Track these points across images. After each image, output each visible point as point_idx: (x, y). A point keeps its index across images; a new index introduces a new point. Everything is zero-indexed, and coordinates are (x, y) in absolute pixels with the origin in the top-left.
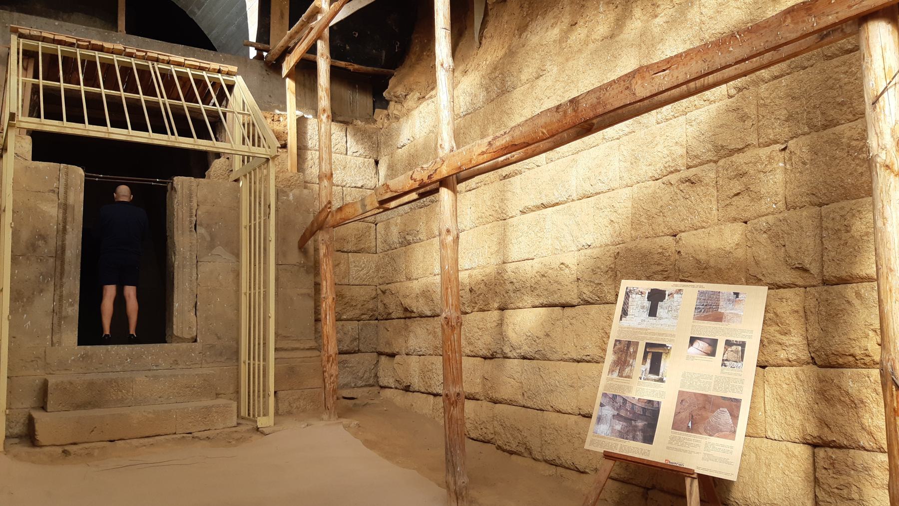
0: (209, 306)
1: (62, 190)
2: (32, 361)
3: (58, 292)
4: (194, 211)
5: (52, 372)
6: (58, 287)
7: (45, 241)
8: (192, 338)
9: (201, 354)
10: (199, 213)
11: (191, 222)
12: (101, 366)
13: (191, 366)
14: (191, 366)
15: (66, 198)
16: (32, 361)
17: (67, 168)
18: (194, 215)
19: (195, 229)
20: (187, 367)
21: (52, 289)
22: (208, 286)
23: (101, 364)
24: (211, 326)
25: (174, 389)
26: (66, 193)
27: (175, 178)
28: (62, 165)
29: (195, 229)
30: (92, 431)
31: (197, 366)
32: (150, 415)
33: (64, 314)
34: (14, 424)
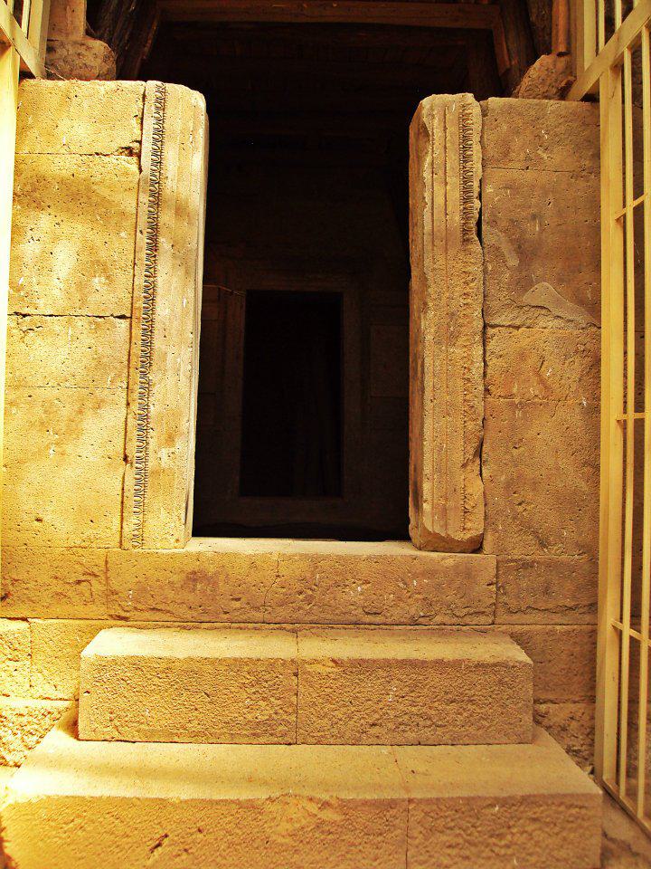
0: (515, 452)
1: (147, 148)
2: (79, 582)
3: (135, 407)
4: (476, 184)
5: (123, 614)
6: (136, 396)
7: (108, 277)
8: (471, 540)
9: (493, 588)
10: (489, 190)
11: (466, 215)
12: (237, 604)
13: (467, 620)
14: (467, 620)
15: (158, 162)
16: (79, 582)
17: (164, 92)
18: (476, 194)
19: (479, 234)
20: (455, 620)
21: (121, 396)
22: (511, 396)
23: (239, 599)
24: (520, 509)
25: (413, 704)
26: (158, 154)
27: (426, 102)
28: (152, 85)
29: (479, 234)
30: (159, 845)
31: (483, 619)
32: (328, 815)
33: (152, 464)
34: (35, 738)
